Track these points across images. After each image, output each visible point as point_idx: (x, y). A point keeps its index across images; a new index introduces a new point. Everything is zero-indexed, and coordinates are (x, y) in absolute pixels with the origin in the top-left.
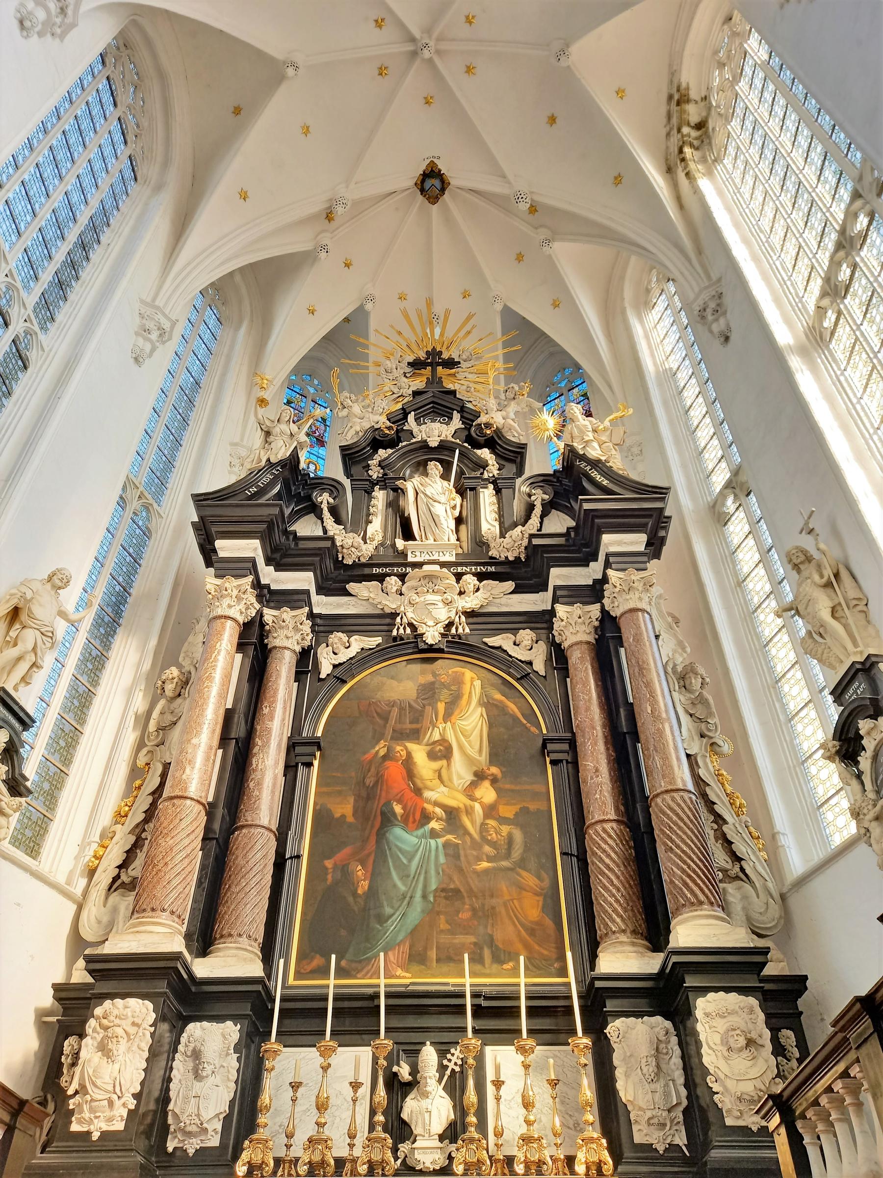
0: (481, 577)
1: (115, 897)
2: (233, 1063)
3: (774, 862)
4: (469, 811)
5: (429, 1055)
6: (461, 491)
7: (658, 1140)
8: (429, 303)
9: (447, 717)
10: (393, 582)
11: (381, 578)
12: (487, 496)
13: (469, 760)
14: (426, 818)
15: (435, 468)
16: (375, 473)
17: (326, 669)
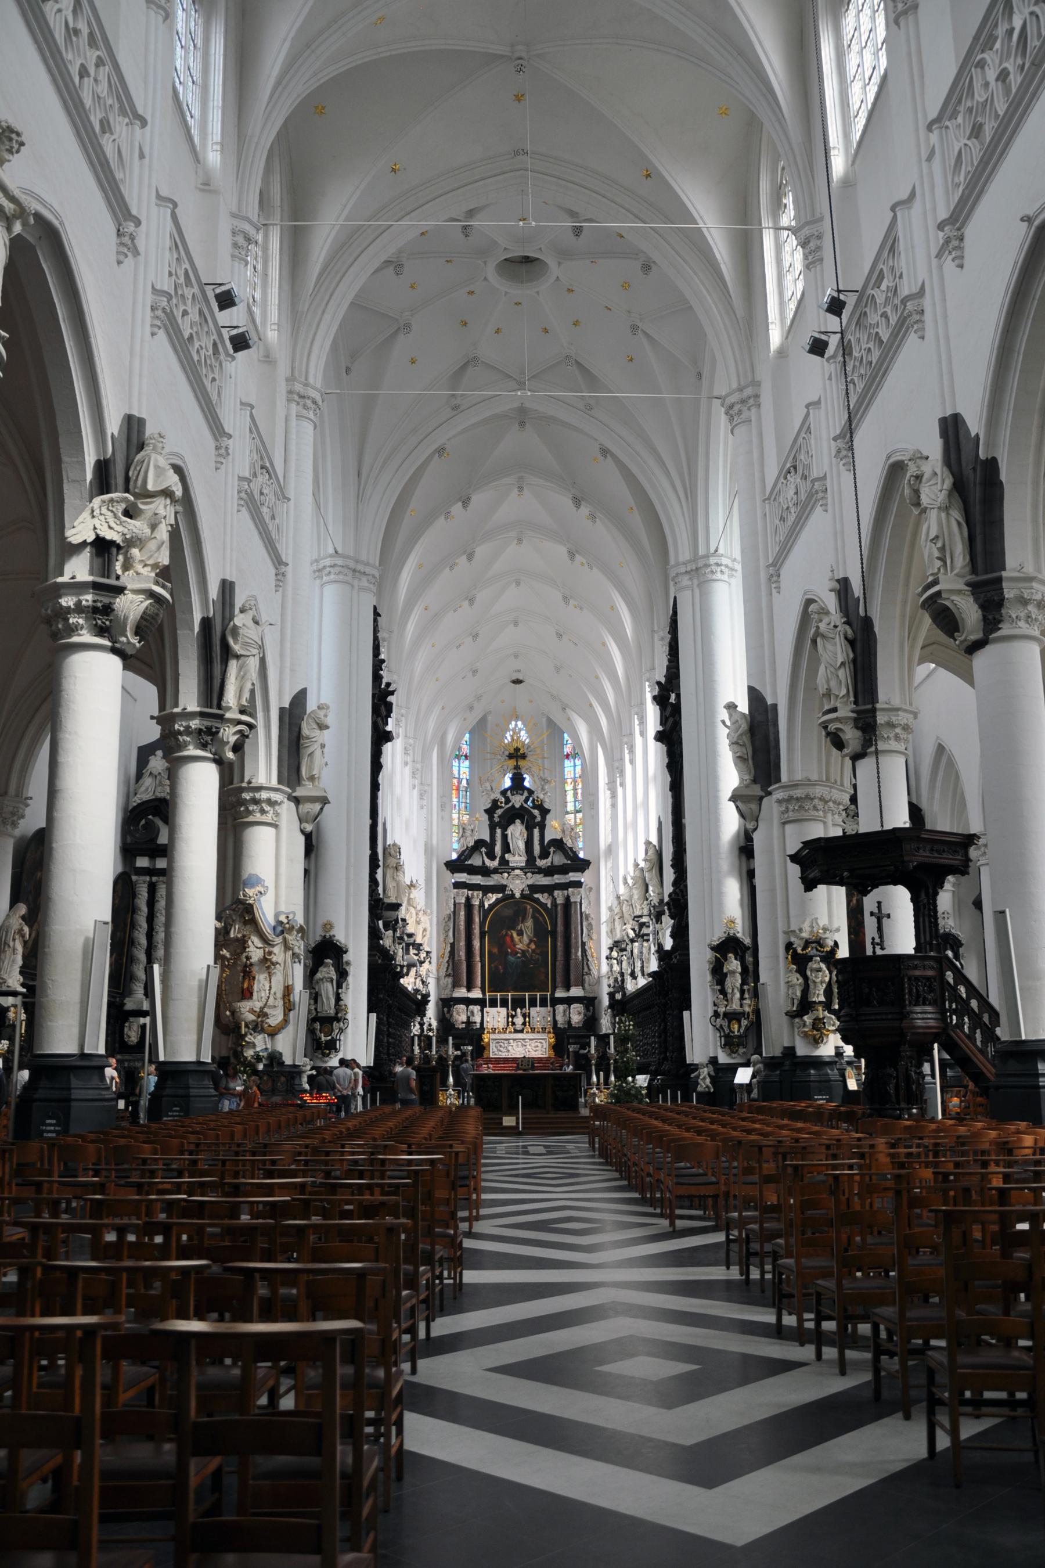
0: (533, 873)
1: (447, 979)
2: (480, 1013)
3: (599, 970)
4: (528, 951)
5: (519, 1010)
6: (527, 828)
7: (562, 1026)
8: (515, 708)
9: (522, 922)
10: (506, 875)
11: (501, 873)
12: (536, 832)
13: (528, 936)
14: (517, 953)
15: (518, 821)
16: (496, 819)
17: (486, 906)
